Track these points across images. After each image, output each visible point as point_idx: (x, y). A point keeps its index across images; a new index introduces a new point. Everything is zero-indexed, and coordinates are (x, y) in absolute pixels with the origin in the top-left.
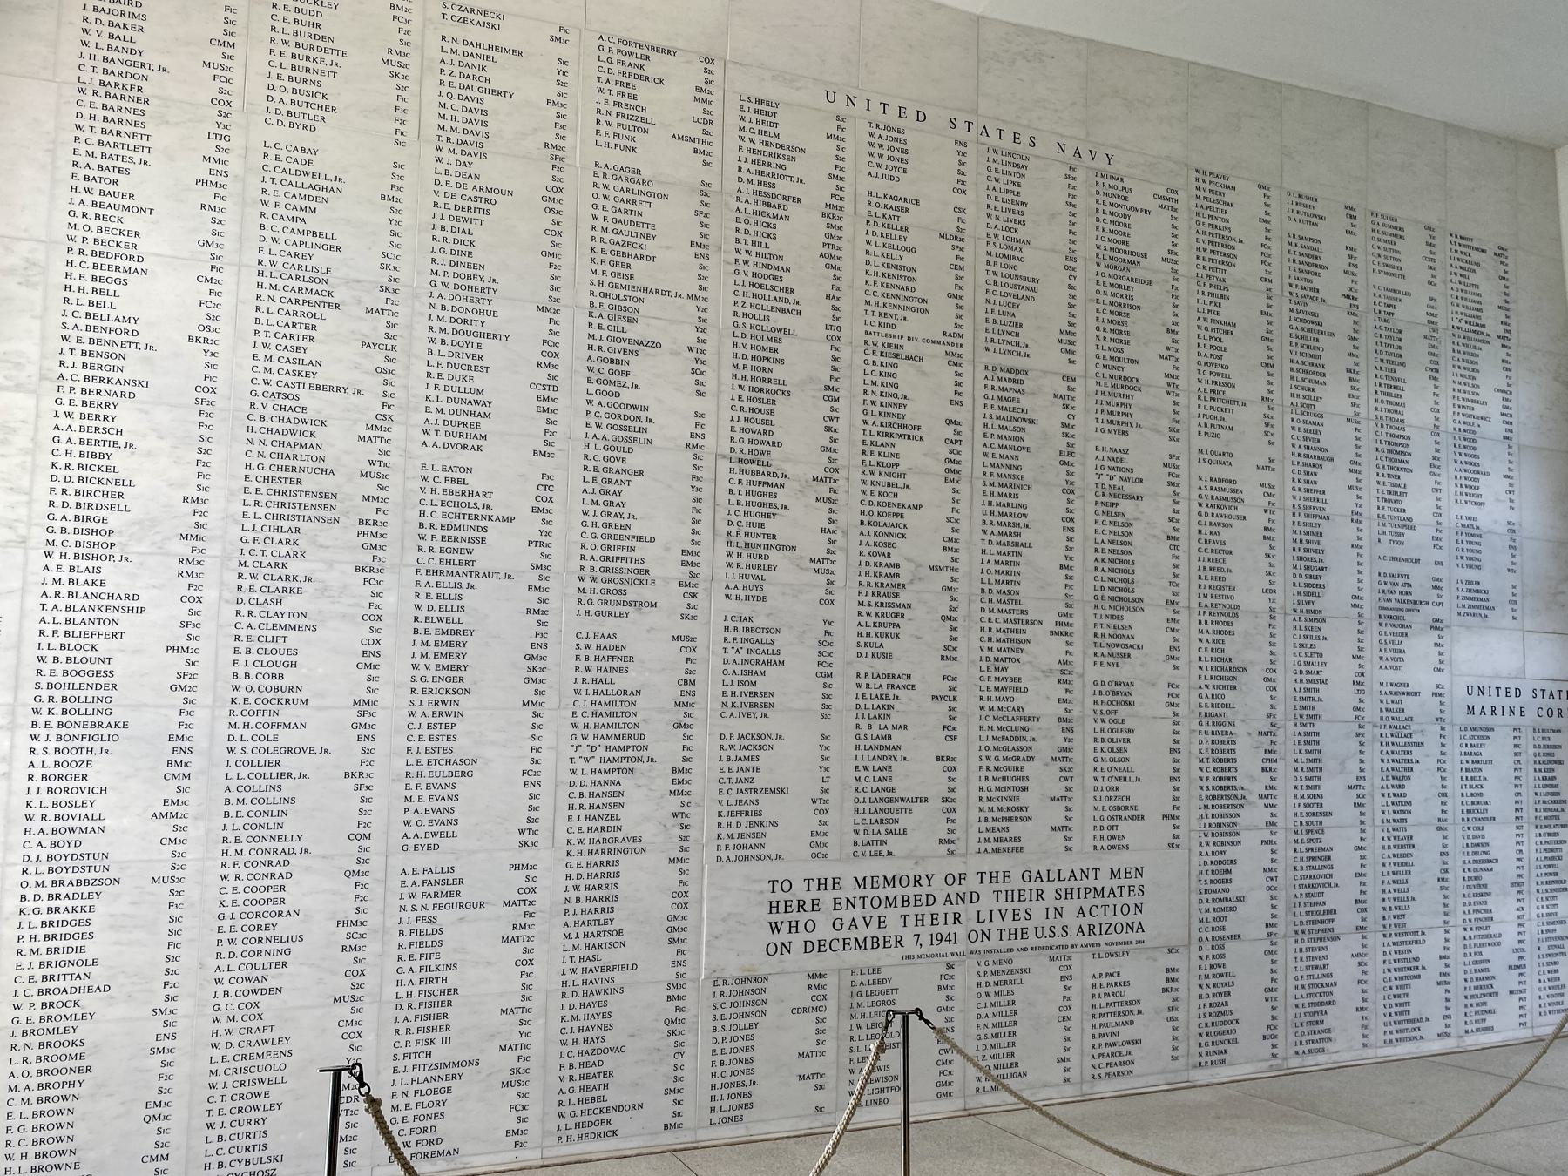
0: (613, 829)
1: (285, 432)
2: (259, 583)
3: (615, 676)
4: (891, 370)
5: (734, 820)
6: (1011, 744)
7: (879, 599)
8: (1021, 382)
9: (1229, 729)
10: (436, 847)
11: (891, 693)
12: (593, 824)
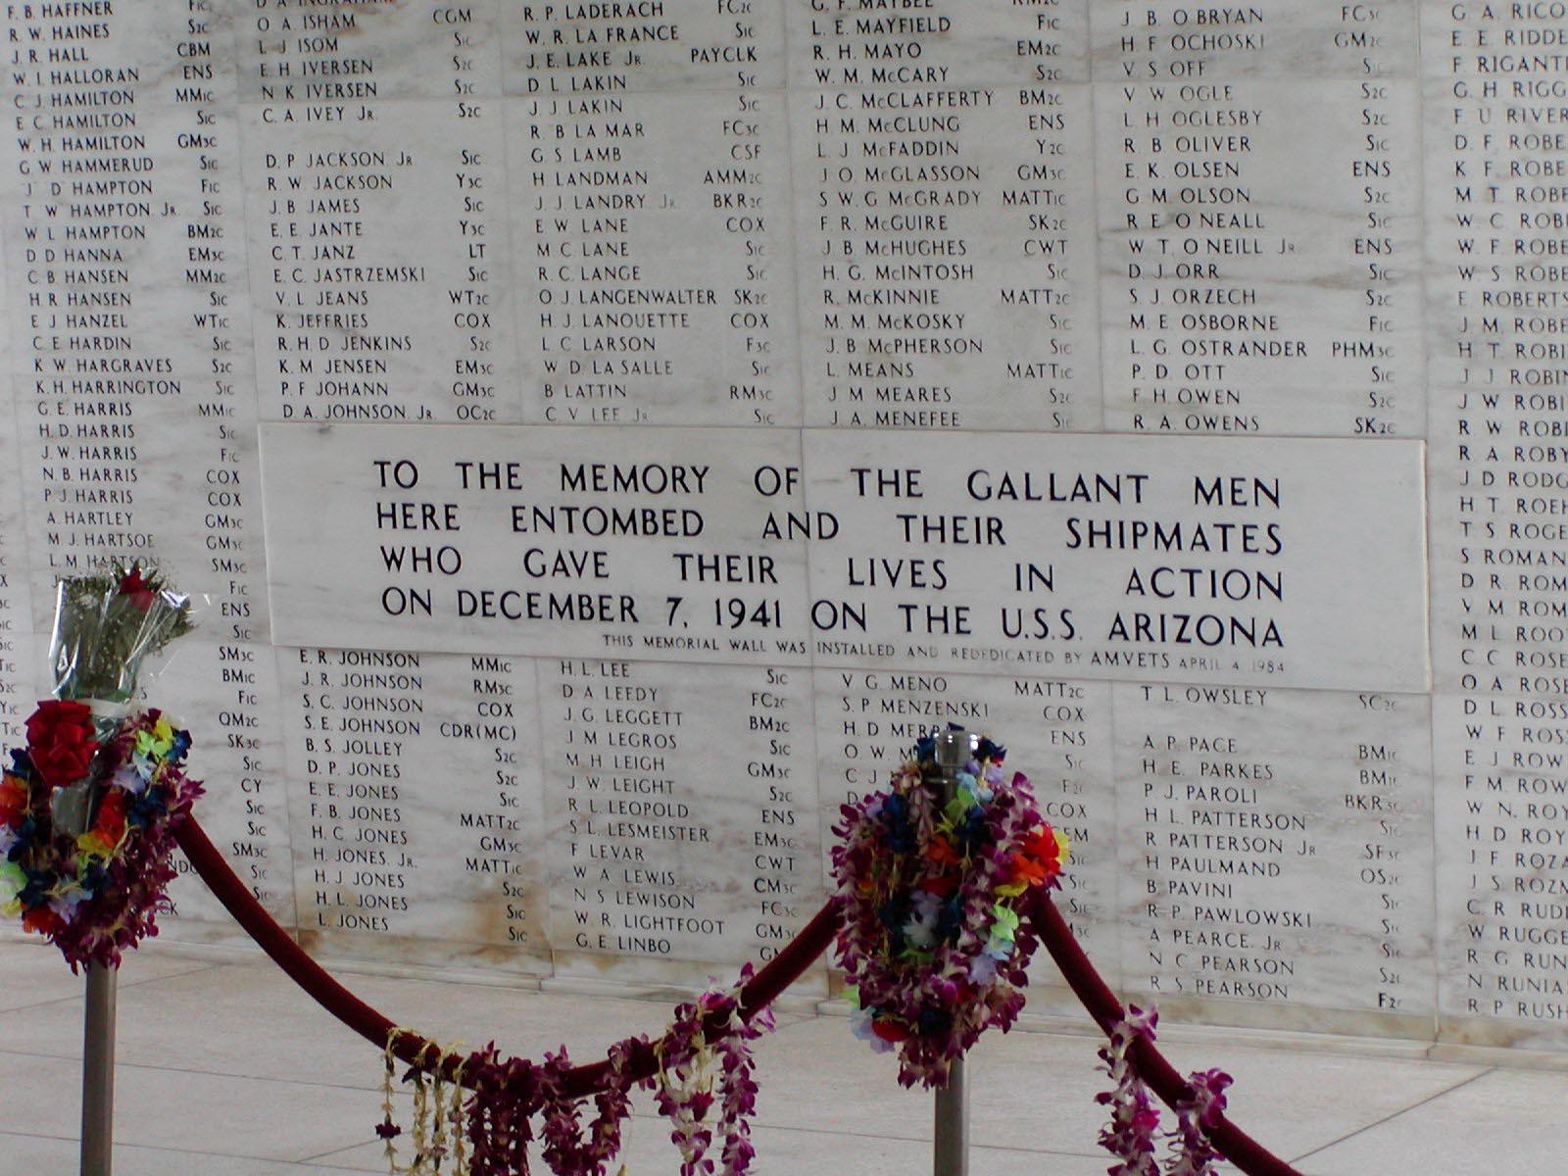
0: (112, 343)
3: (84, 42)
5: (313, 334)
6: (913, 163)
11: (620, 50)
12: (81, 333)
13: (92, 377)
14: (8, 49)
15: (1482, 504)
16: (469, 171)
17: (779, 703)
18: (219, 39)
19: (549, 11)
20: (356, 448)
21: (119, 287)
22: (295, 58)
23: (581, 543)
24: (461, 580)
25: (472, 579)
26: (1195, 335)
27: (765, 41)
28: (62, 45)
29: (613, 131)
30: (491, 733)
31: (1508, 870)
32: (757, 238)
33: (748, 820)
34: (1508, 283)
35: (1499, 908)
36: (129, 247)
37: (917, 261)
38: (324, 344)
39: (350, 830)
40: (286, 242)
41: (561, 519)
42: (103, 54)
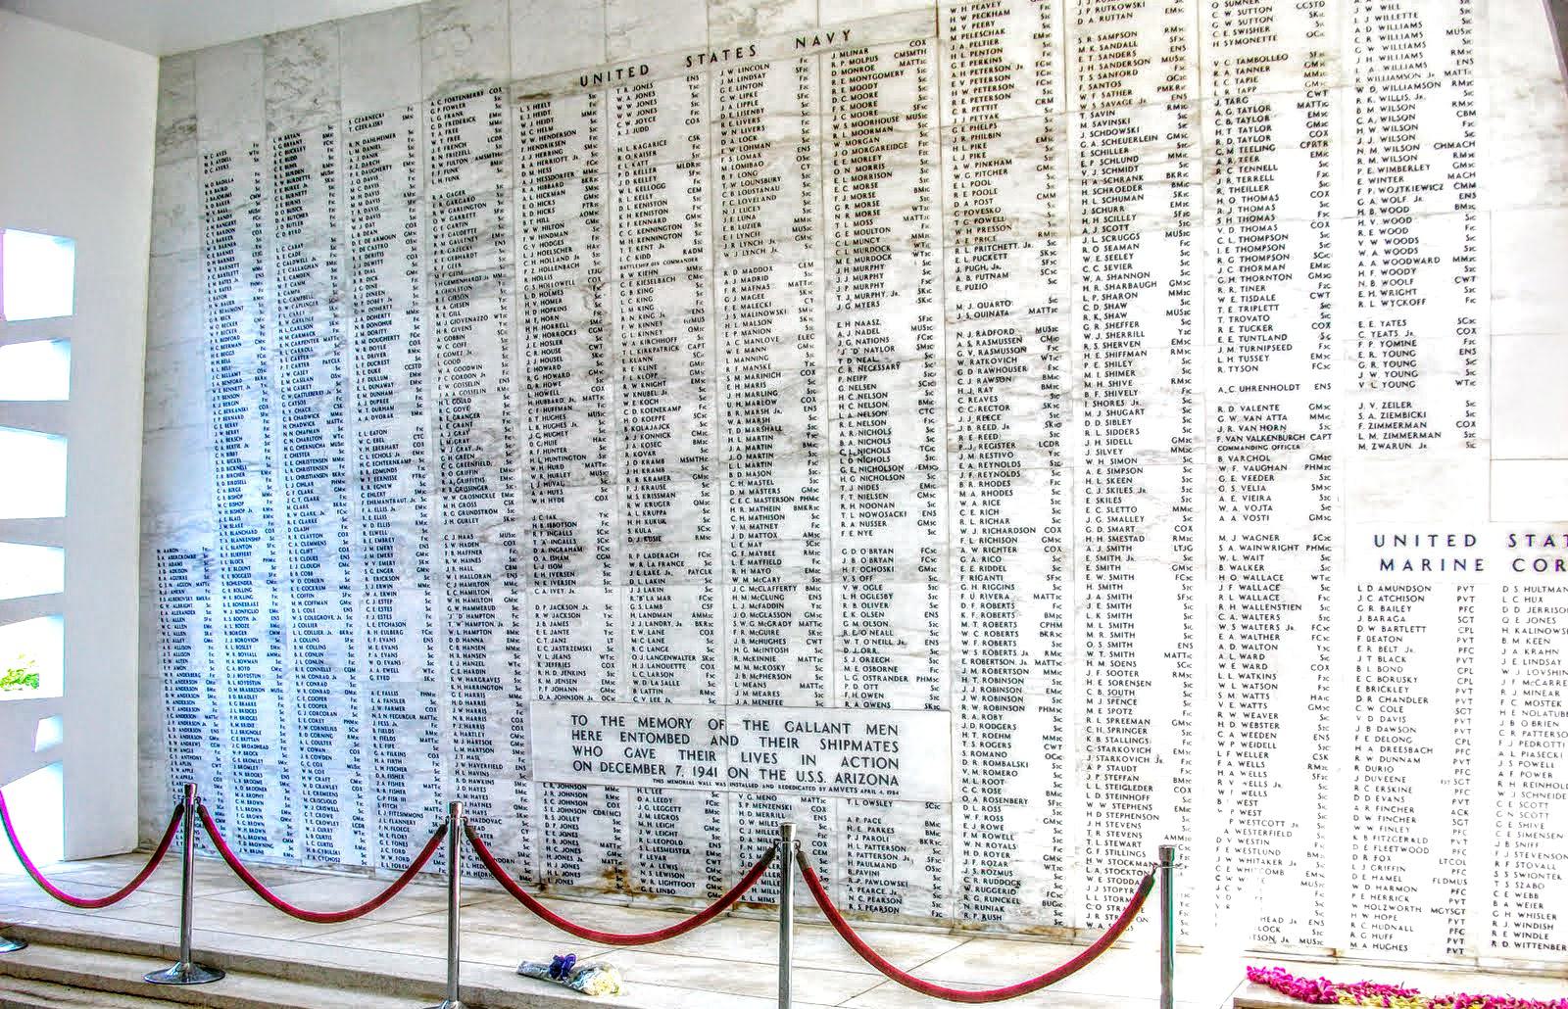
1: (301, 425)
2: (299, 517)
4: (647, 295)
5: (551, 670)
7: (646, 492)
8: (766, 278)
10: (388, 678)
11: (662, 570)
13: (472, 684)
14: (445, 566)
15: (971, 735)
17: (716, 804)
18: (520, 564)
20: (564, 711)
21: (482, 652)
22: (547, 571)
23: (644, 745)
25: (606, 758)
26: (868, 674)
27: (716, 566)
28: (464, 565)
30: (612, 814)
31: (979, 868)
32: (710, 637)
33: (705, 846)
34: (980, 656)
35: (975, 880)
36: (485, 637)
38: (555, 673)
39: (560, 847)
40: (542, 637)
42: (478, 568)
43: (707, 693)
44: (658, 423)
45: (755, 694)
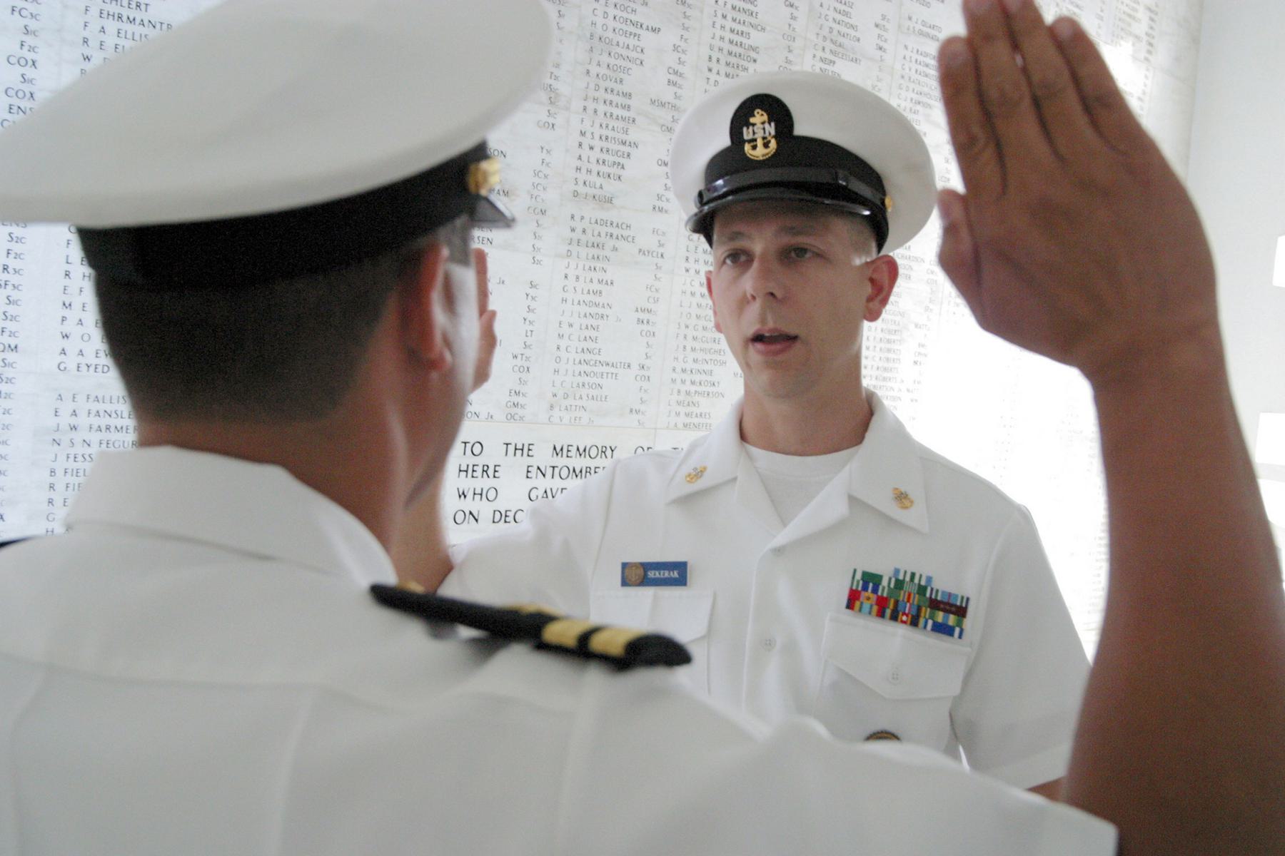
7: (605, 132)
9: (898, 318)
11: (611, 243)
16: (532, 292)
19: (582, 218)
24: (495, 506)
25: (501, 505)
29: (600, 282)
37: (708, 357)
41: (549, 472)
43: (637, 412)
44: (632, 42)
45: (687, 415)
